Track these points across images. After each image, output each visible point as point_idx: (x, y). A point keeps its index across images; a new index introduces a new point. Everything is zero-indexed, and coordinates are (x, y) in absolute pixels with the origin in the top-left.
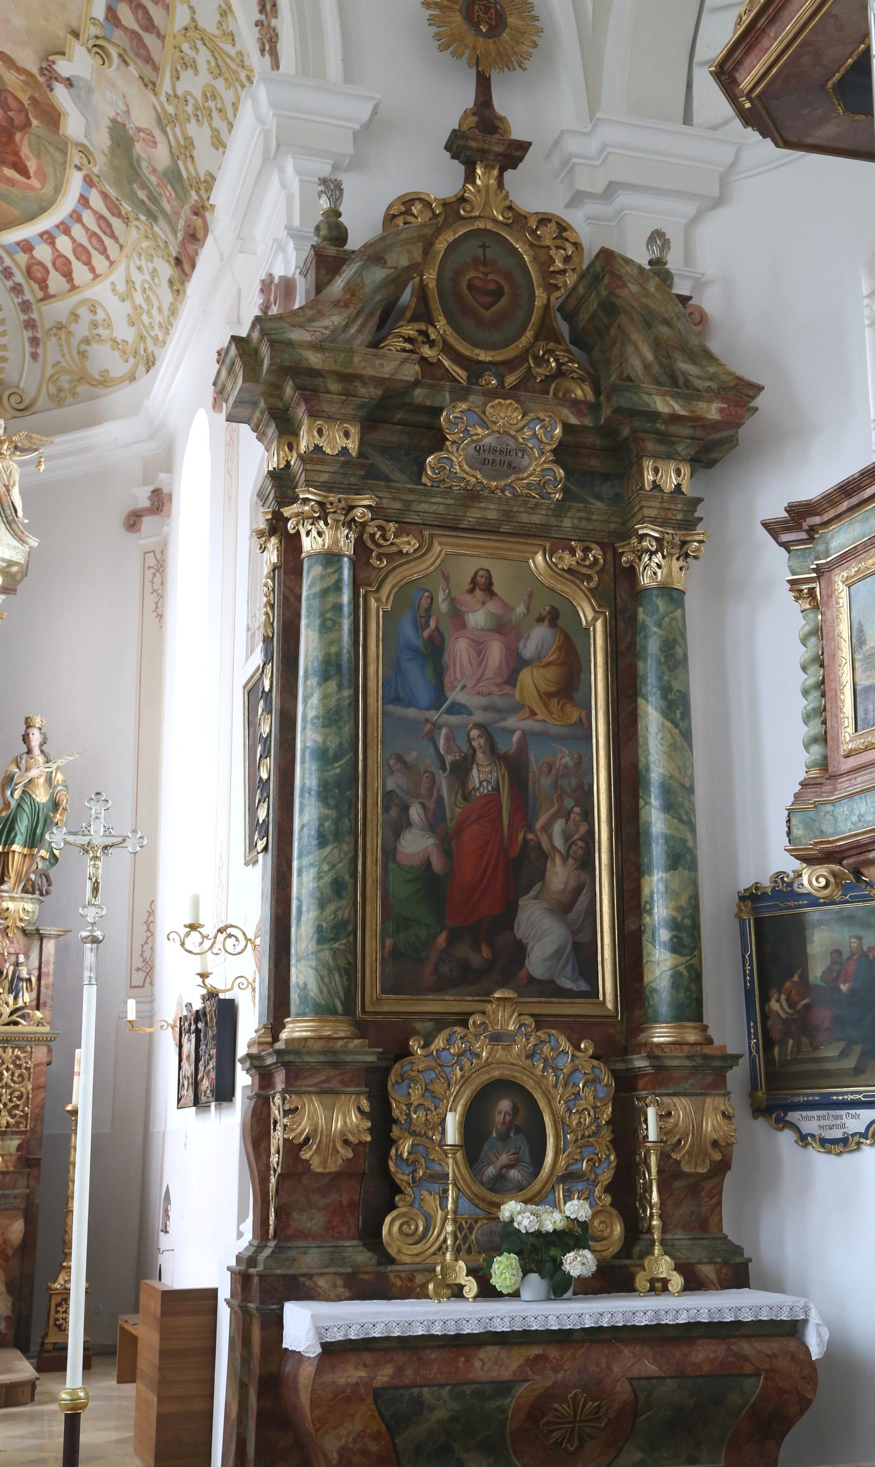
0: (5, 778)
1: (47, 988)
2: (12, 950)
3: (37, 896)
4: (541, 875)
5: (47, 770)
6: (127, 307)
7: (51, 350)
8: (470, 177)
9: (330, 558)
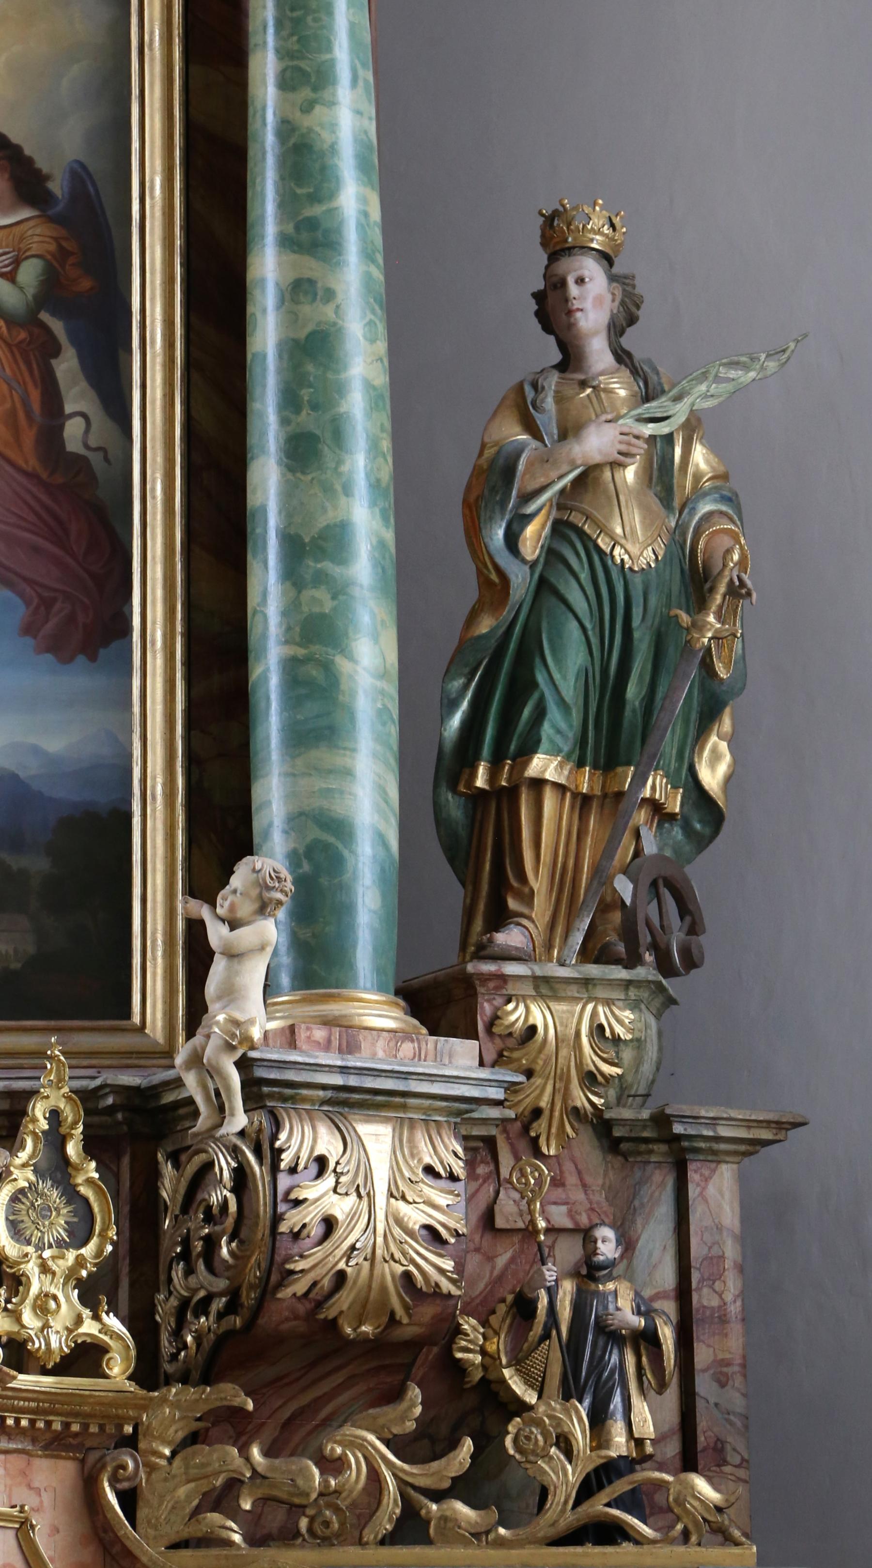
0: (478, 472)
1: (722, 1382)
2: (560, 1216)
3: (646, 972)
5: (649, 429)
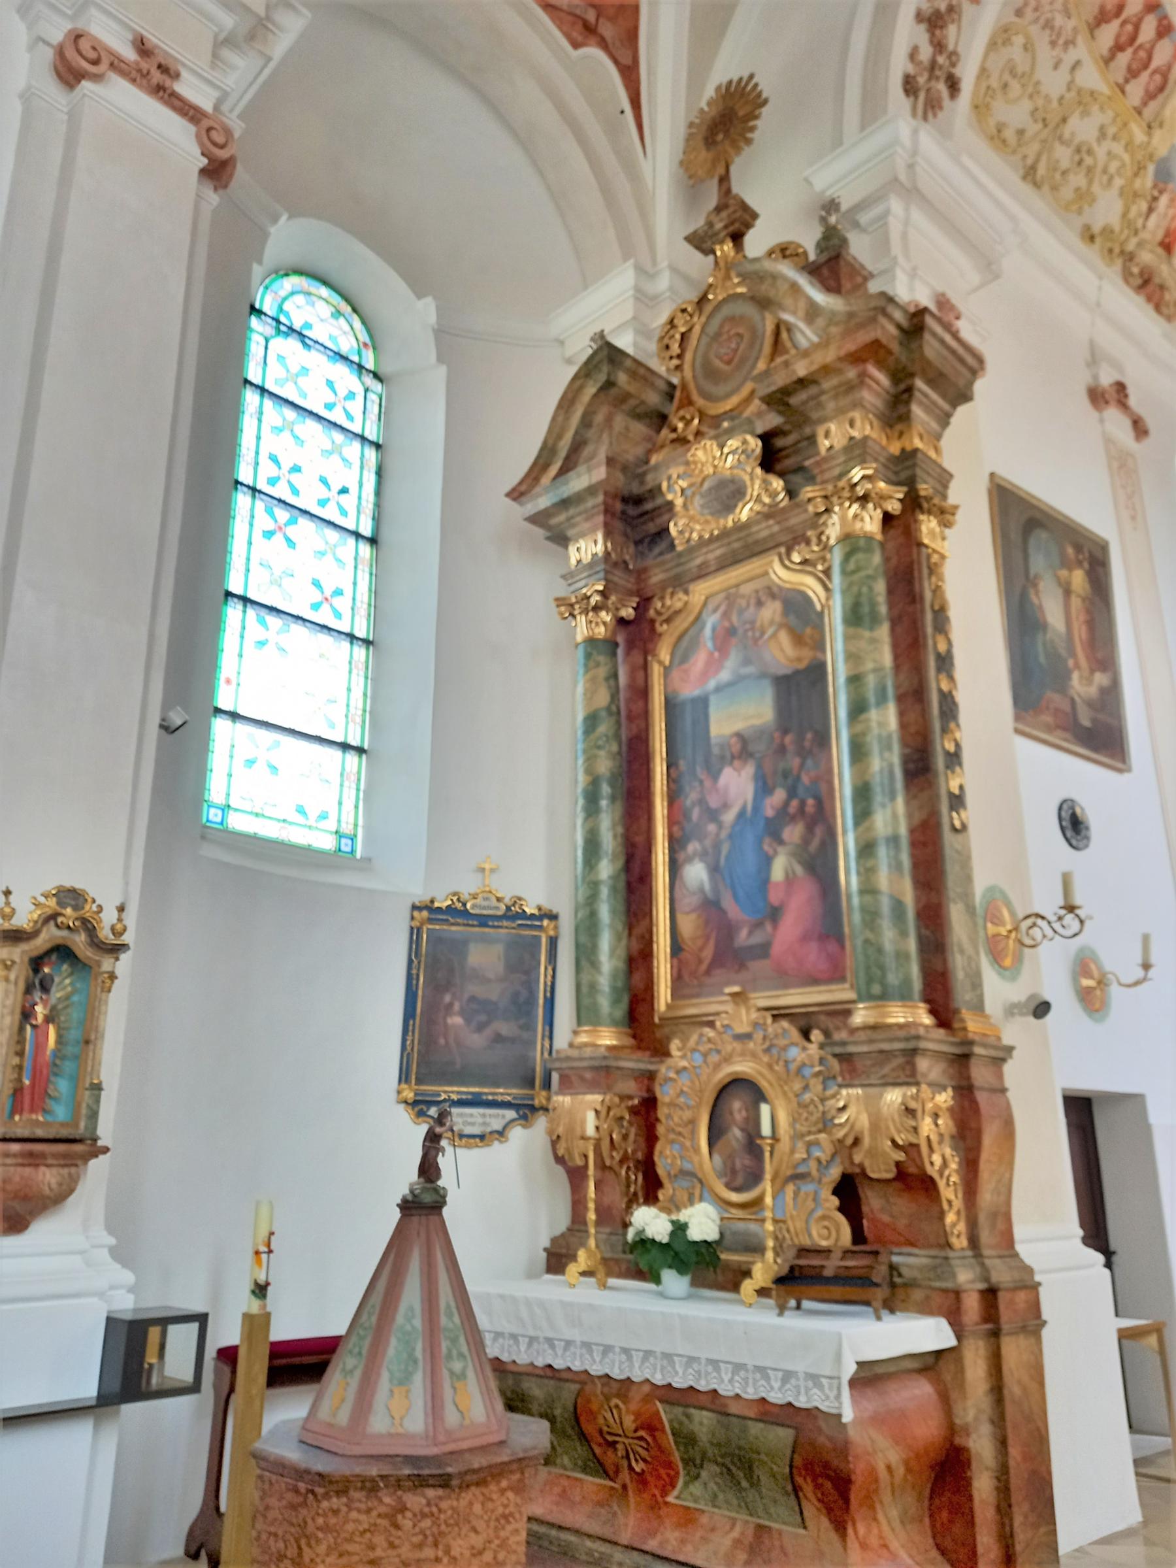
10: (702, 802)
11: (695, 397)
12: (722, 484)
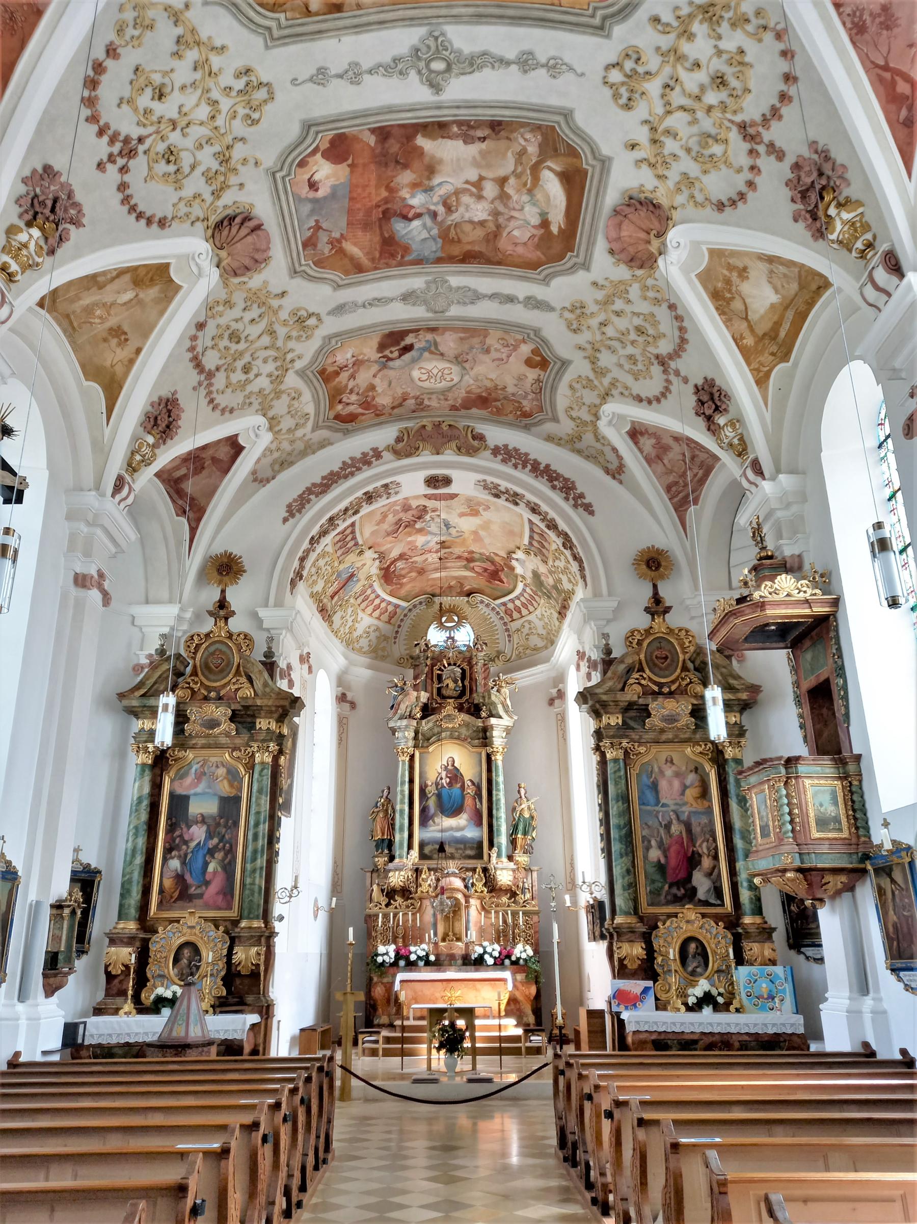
4: (699, 863)
6: (542, 623)
7: (515, 637)
8: (653, 620)
9: (616, 760)
10: (181, 836)
11: (200, 674)
12: (212, 720)
